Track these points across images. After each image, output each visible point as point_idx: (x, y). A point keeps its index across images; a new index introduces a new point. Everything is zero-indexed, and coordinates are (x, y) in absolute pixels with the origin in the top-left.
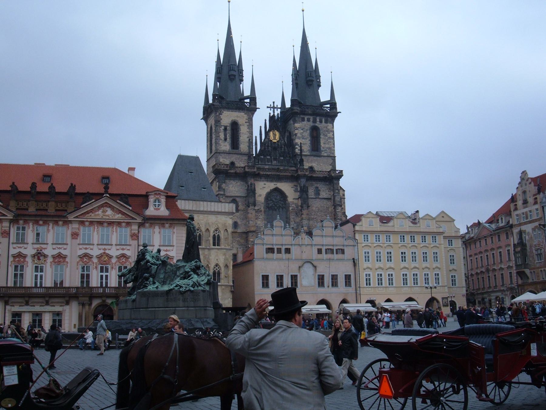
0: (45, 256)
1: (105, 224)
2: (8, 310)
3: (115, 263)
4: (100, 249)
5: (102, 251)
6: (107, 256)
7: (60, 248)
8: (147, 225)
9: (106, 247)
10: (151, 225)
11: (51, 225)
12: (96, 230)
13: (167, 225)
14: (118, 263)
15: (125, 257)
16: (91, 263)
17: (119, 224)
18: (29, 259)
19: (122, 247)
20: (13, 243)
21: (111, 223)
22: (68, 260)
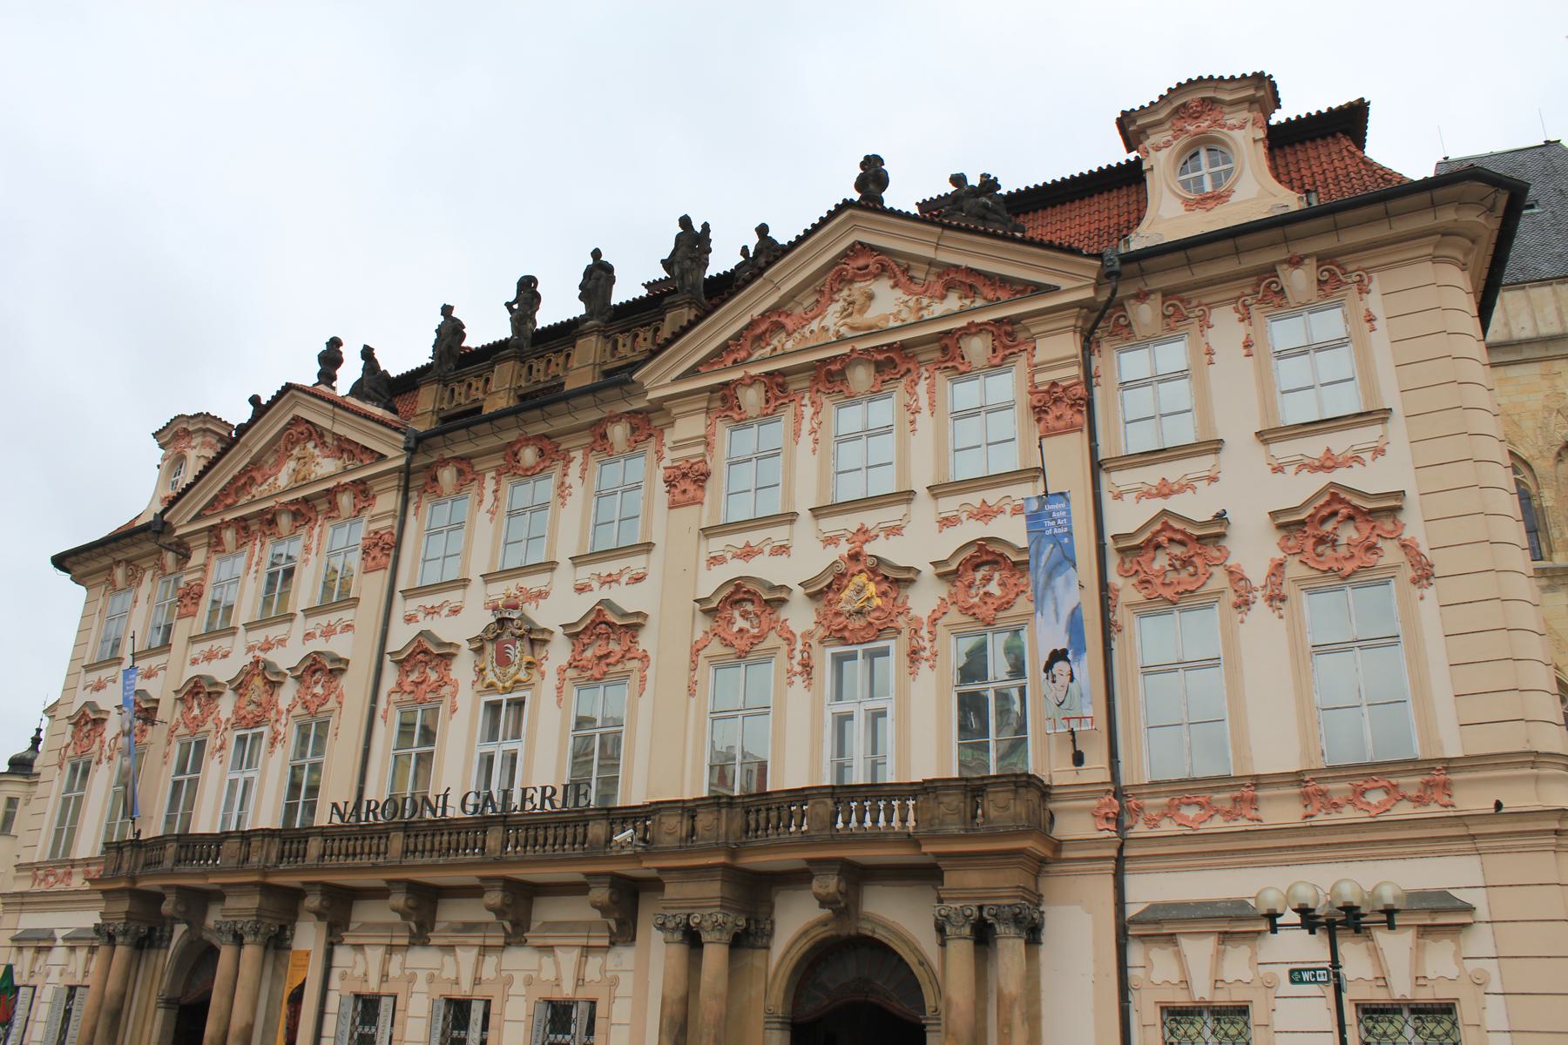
0: (535, 638)
1: (861, 377)
2: (343, 977)
3: (934, 622)
4: (830, 541)
5: (844, 549)
6: (873, 571)
7: (610, 580)
8: (1145, 314)
9: (871, 519)
10: (1181, 311)
11: (578, 455)
12: (806, 426)
13: (1299, 280)
14: (954, 616)
15: (997, 561)
16: (773, 640)
17: (946, 349)
18: (463, 669)
19: (975, 499)
20: (408, 594)
21: (893, 361)
22: (646, 641)
